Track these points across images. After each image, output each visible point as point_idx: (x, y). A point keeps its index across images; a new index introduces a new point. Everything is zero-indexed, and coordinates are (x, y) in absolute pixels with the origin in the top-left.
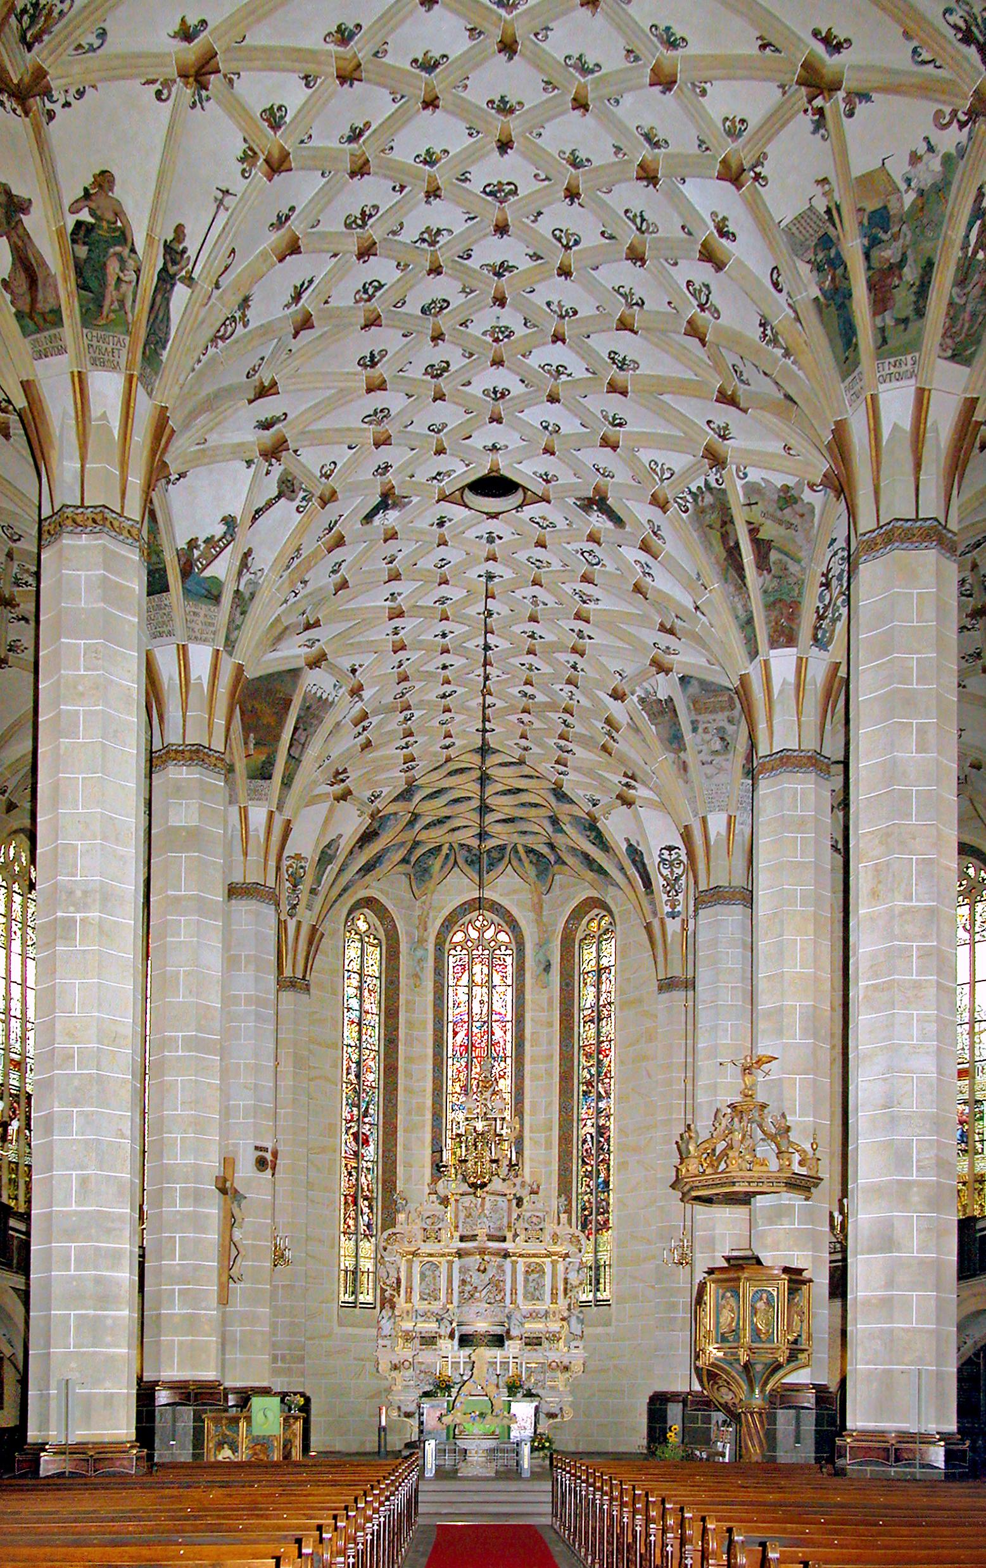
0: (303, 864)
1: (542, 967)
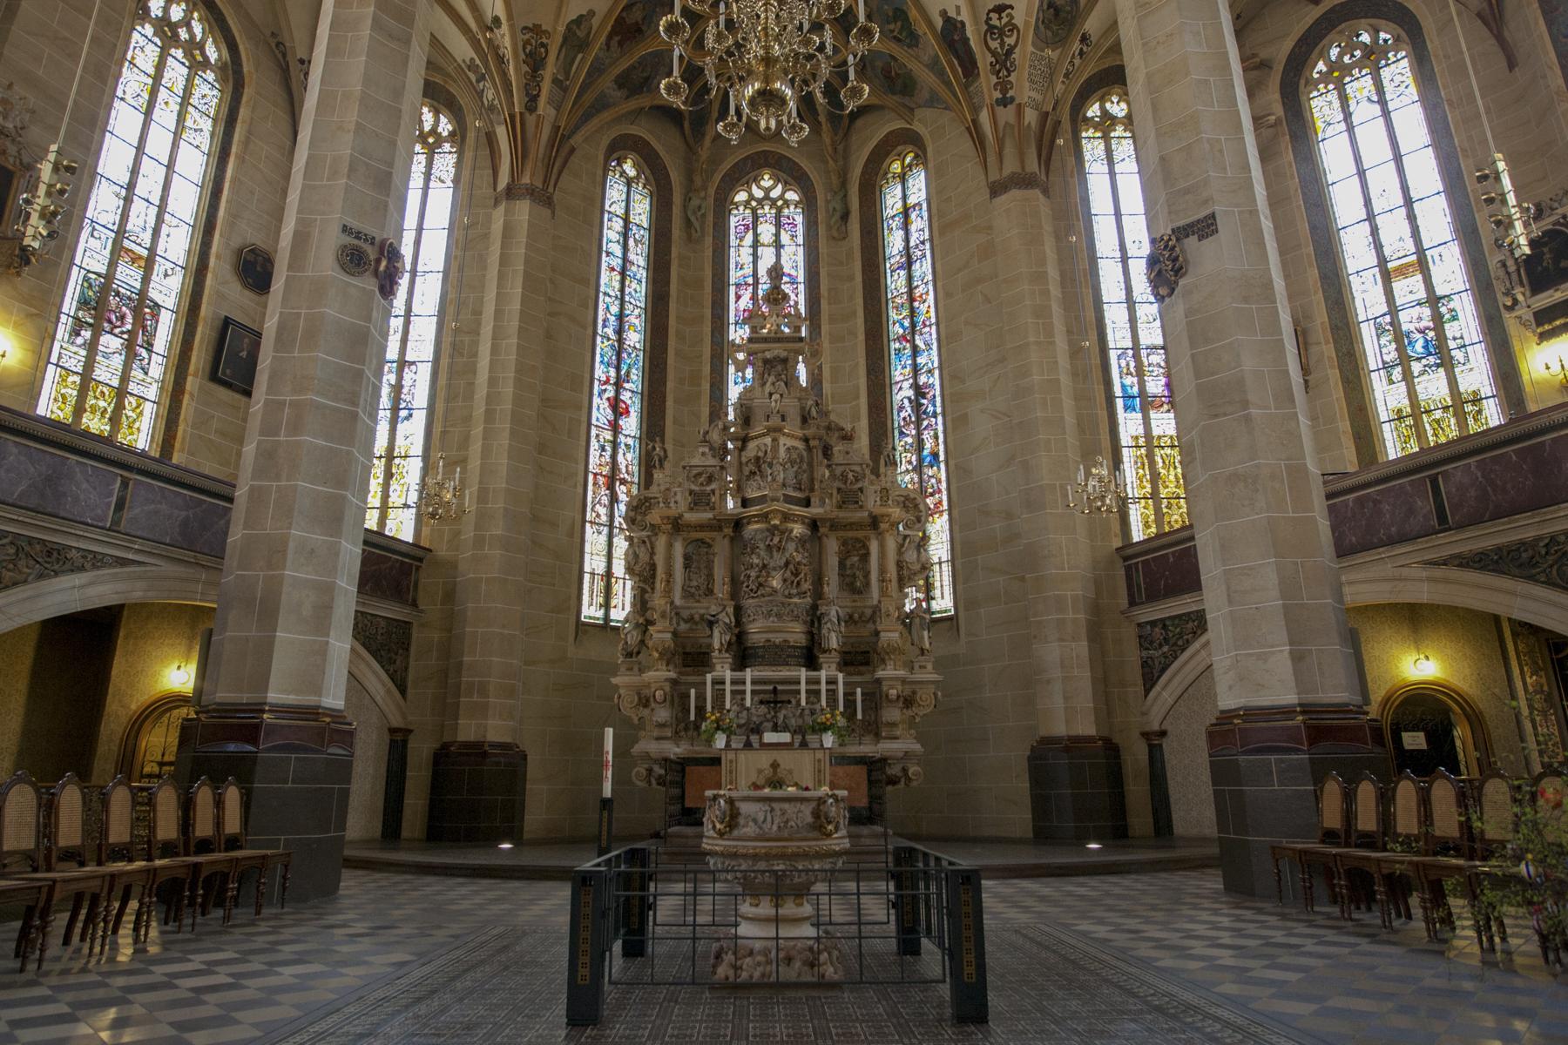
0: (544, 40)
1: (837, 215)
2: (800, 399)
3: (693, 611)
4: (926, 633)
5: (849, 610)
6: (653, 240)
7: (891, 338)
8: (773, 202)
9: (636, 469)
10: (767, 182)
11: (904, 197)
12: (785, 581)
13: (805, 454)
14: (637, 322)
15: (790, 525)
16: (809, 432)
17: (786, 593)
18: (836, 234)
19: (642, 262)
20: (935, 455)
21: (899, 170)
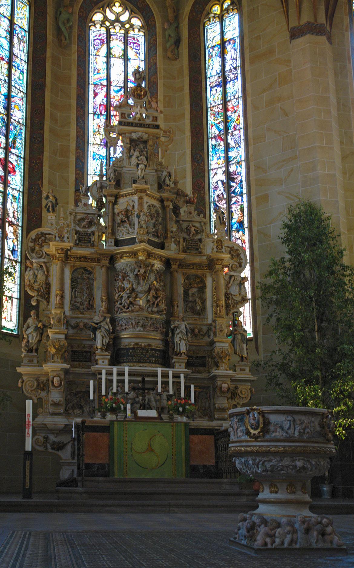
1: (172, 40)
2: (156, 171)
3: (79, 320)
4: (245, 345)
5: (192, 327)
6: (31, 41)
7: (210, 136)
8: (123, 24)
9: (20, 215)
10: (117, 8)
11: (222, 33)
12: (148, 301)
13: (160, 211)
14: (20, 103)
15: (152, 261)
16: (165, 195)
17: (150, 309)
18: (170, 55)
19: (24, 57)
20: (241, 223)
21: (218, 12)
